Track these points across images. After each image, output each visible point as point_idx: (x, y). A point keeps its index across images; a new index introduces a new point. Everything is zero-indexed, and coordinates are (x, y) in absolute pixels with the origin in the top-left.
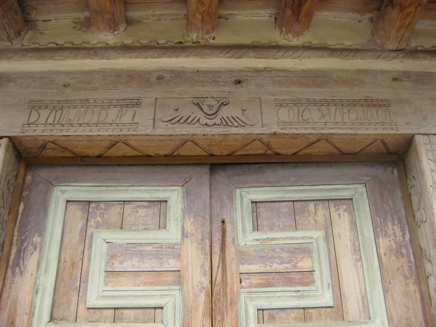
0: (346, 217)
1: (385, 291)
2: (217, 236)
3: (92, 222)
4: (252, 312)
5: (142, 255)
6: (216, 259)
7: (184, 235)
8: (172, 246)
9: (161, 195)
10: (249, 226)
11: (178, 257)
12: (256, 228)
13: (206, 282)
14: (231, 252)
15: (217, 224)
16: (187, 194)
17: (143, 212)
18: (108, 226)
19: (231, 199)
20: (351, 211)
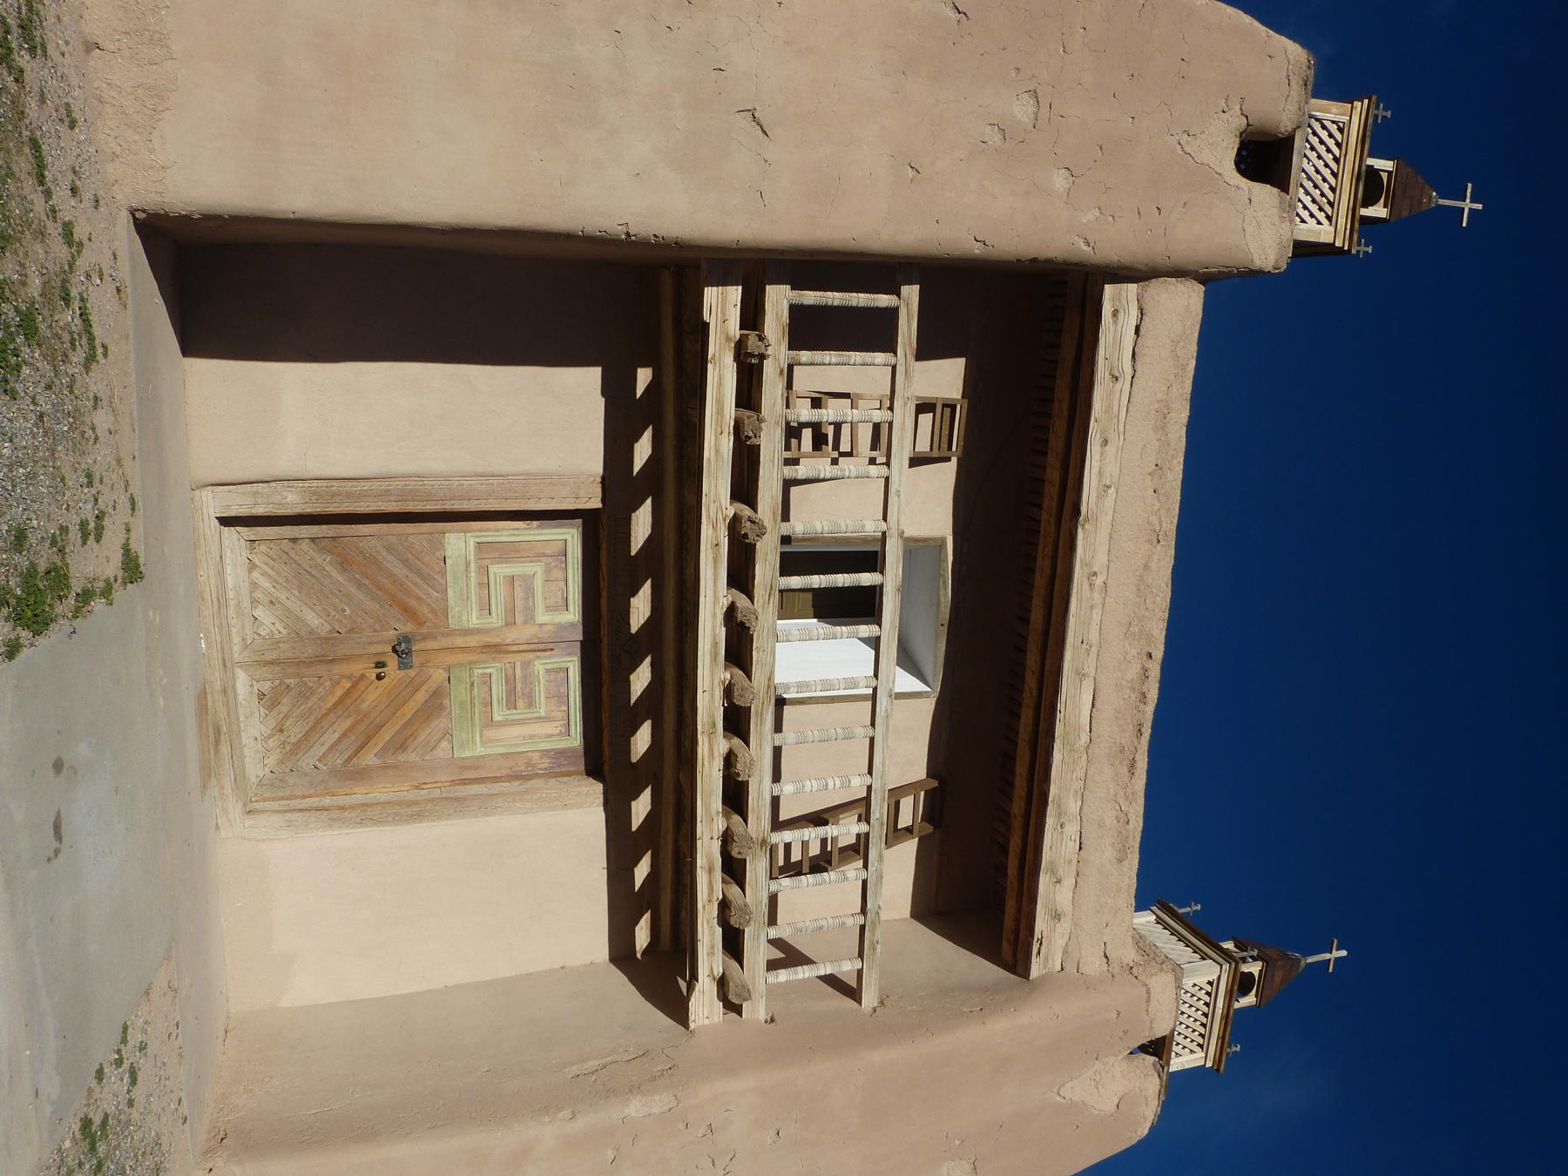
0: (557, 731)
1: (502, 754)
2: (542, 646)
3: (550, 560)
4: (488, 671)
5: (526, 599)
6: (522, 648)
7: (541, 625)
8: (533, 618)
9: (571, 607)
10: (548, 667)
11: (526, 622)
12: (547, 671)
13: (508, 641)
14: (531, 656)
15: (551, 646)
16: (572, 625)
17: (559, 594)
18: (548, 571)
19: (570, 654)
20: (561, 734)
